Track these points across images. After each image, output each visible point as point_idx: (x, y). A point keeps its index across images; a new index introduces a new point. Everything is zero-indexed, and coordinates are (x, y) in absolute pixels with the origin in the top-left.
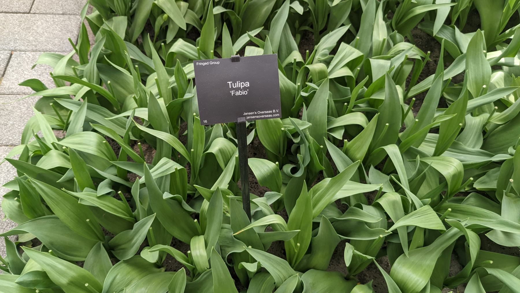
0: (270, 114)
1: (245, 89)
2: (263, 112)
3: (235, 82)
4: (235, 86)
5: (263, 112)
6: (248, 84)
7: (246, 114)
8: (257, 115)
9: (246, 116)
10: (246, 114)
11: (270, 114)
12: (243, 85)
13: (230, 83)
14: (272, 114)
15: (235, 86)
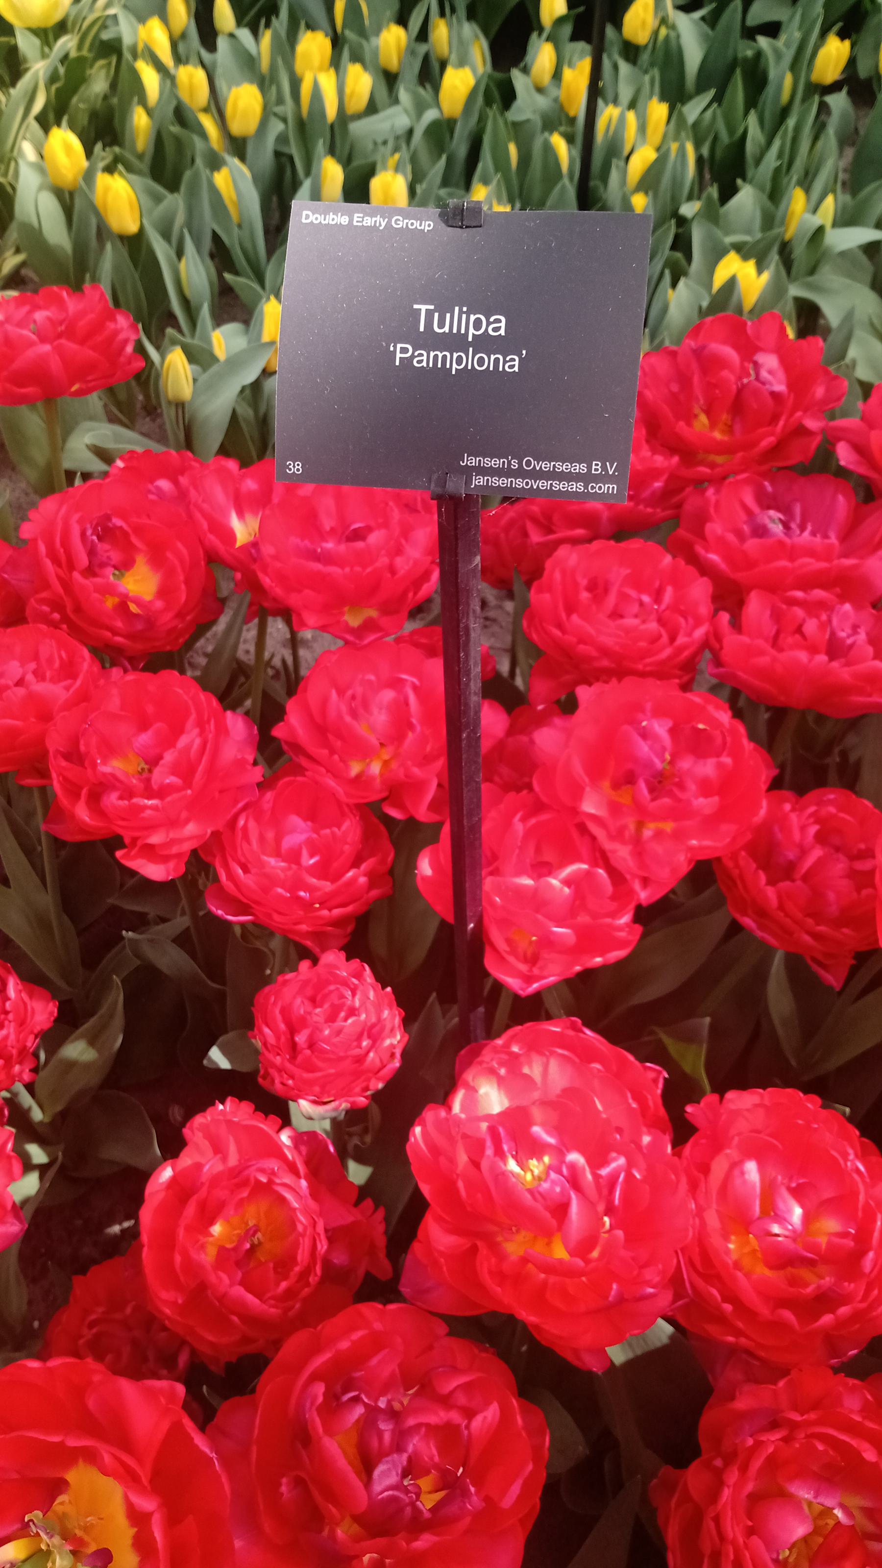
0: (577, 477)
1: (484, 344)
2: (546, 466)
3: (444, 308)
4: (441, 325)
5: (546, 466)
6: (499, 326)
7: (473, 461)
8: (520, 473)
9: (469, 471)
10: (473, 461)
11: (577, 477)
12: (478, 324)
13: (423, 308)
14: (587, 478)
15: (441, 325)
